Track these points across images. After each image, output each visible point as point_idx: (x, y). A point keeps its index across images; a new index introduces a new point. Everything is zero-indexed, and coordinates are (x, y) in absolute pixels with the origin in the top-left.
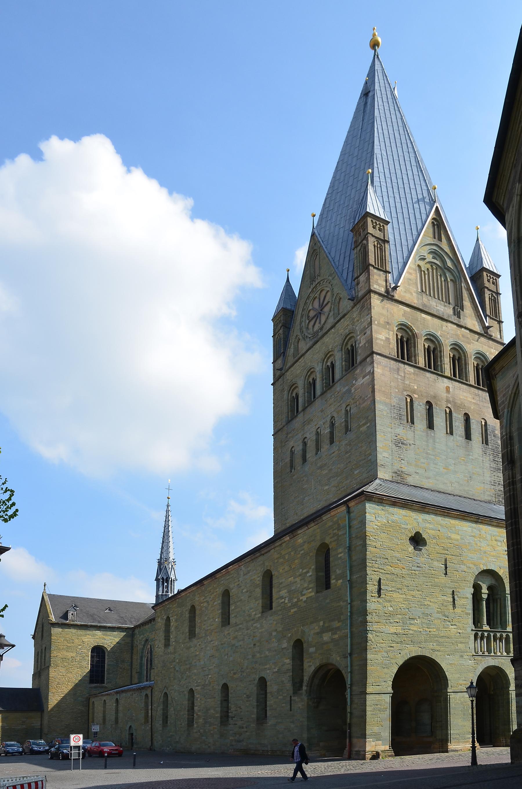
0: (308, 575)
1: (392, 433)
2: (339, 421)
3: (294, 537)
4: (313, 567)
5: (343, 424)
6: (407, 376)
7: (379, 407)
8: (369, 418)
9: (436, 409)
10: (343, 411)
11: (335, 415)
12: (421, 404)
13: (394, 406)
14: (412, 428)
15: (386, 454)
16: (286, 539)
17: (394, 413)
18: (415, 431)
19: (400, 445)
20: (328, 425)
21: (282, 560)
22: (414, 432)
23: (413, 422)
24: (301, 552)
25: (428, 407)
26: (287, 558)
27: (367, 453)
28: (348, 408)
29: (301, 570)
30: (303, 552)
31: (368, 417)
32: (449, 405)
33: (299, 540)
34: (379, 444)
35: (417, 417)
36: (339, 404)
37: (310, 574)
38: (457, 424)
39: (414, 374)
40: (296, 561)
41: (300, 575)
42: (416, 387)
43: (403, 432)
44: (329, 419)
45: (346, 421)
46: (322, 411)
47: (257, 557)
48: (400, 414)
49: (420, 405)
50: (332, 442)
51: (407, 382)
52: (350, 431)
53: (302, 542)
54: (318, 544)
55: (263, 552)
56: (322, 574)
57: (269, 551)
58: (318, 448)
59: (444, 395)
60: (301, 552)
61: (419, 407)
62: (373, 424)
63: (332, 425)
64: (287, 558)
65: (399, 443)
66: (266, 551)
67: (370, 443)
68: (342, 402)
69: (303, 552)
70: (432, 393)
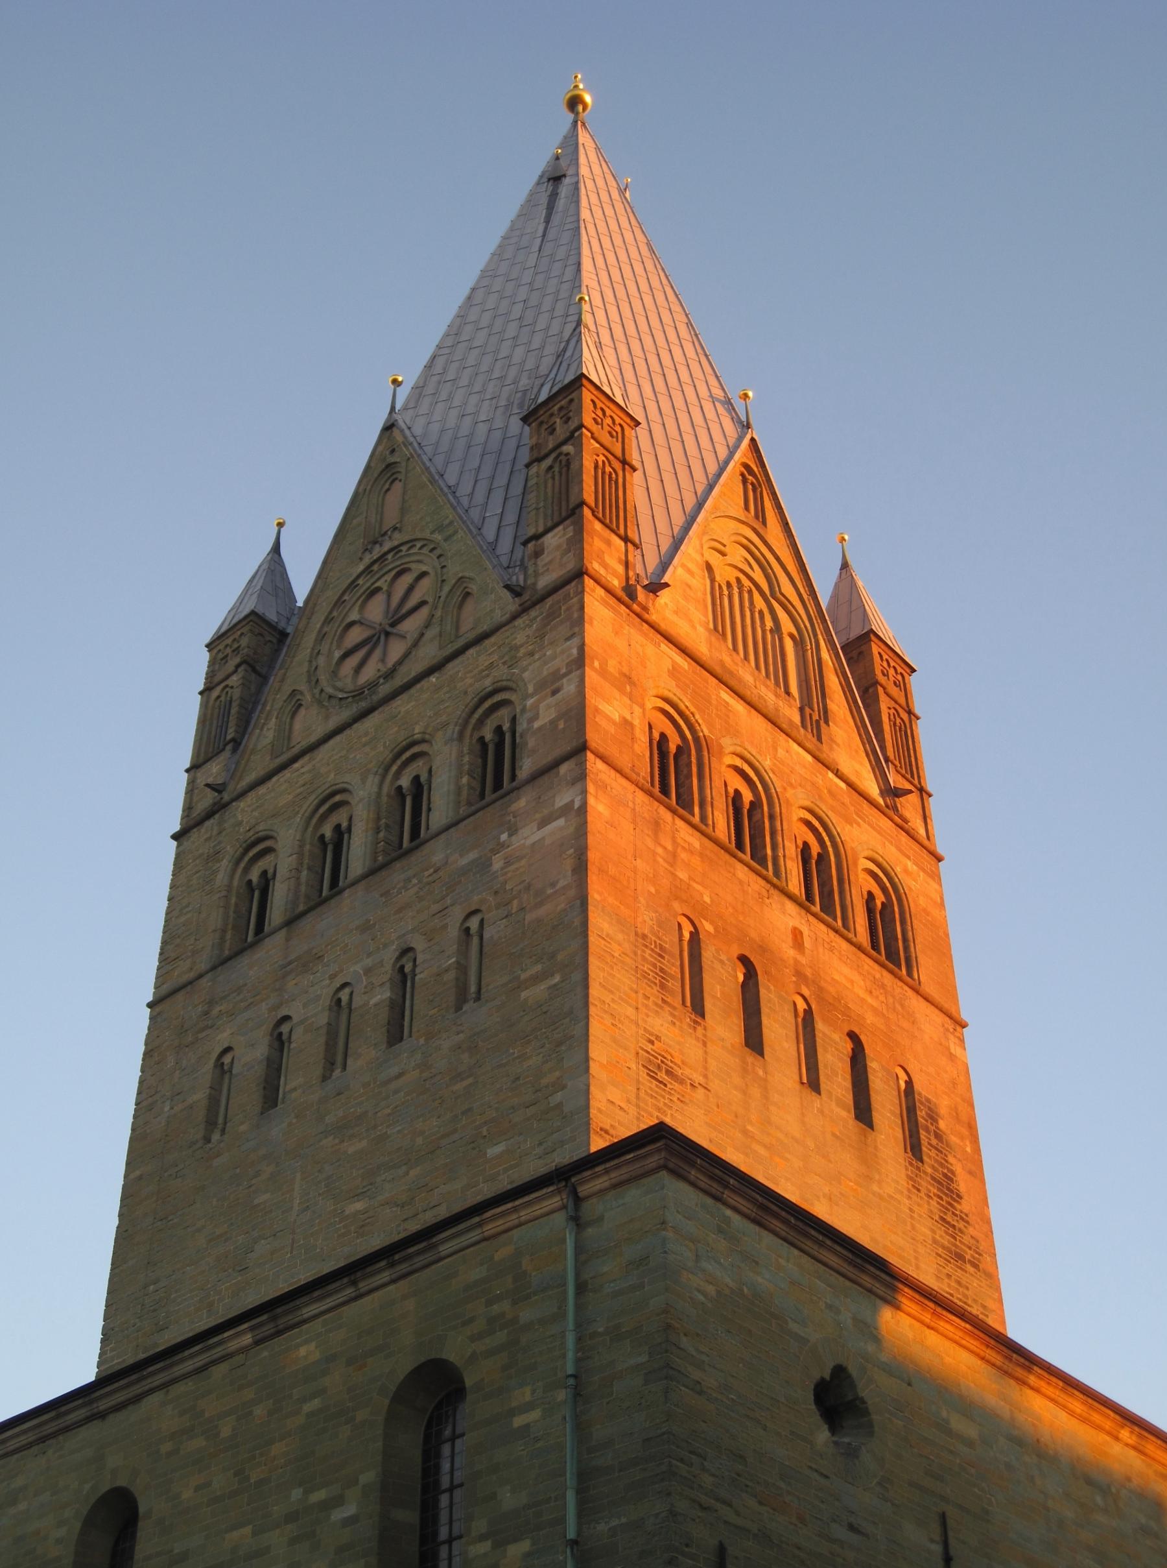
0: (338, 1515)
1: (637, 1025)
2: (435, 963)
3: (279, 1333)
4: (369, 1477)
5: (451, 975)
6: (683, 855)
7: (600, 923)
8: (560, 957)
9: (768, 989)
10: (454, 932)
11: (419, 943)
12: (723, 957)
13: (644, 937)
14: (699, 1029)
15: (615, 1095)
16: (233, 1345)
17: (644, 959)
18: (709, 1044)
19: (662, 1075)
20: (387, 970)
21: (199, 1442)
22: (705, 1044)
23: (698, 1008)
24: (308, 1407)
25: (741, 978)
26: (226, 1431)
27: (544, 1081)
28: (474, 923)
29: (296, 1494)
30: (316, 1403)
31: (553, 956)
32: (806, 992)
33: (303, 1351)
34: (599, 1052)
35: (714, 997)
36: (435, 908)
37: (350, 1510)
38: (829, 1056)
39: (702, 855)
40: (277, 1449)
41: (292, 1517)
42: (707, 899)
43: (670, 1030)
44: (389, 956)
45: (462, 968)
46: (366, 928)
47: (67, 1429)
48: (662, 970)
49: (722, 962)
50: (396, 1033)
51: (682, 875)
52: (478, 998)
53: (317, 1356)
54: (405, 1365)
55: (103, 1405)
56: (409, 1516)
57: (137, 1399)
58: (334, 1056)
59: (790, 953)
60: (308, 1407)
61: (717, 965)
62: (577, 976)
63: (403, 979)
64: (226, 1431)
65: (659, 1067)
66: (120, 1397)
67: (559, 1044)
68: (449, 901)
69: (316, 1403)
70: (753, 934)
